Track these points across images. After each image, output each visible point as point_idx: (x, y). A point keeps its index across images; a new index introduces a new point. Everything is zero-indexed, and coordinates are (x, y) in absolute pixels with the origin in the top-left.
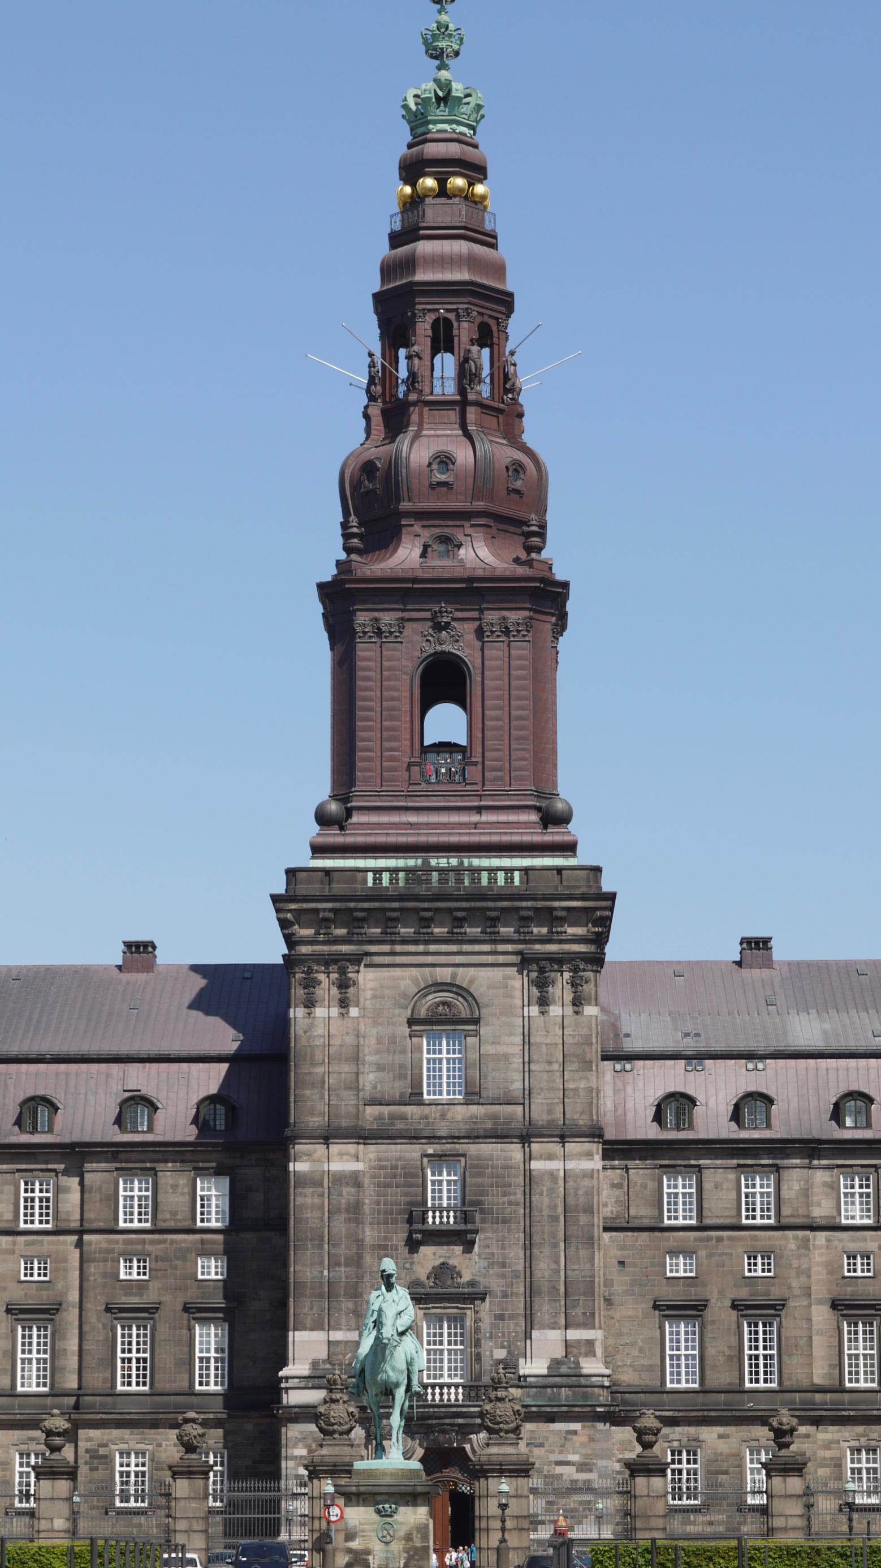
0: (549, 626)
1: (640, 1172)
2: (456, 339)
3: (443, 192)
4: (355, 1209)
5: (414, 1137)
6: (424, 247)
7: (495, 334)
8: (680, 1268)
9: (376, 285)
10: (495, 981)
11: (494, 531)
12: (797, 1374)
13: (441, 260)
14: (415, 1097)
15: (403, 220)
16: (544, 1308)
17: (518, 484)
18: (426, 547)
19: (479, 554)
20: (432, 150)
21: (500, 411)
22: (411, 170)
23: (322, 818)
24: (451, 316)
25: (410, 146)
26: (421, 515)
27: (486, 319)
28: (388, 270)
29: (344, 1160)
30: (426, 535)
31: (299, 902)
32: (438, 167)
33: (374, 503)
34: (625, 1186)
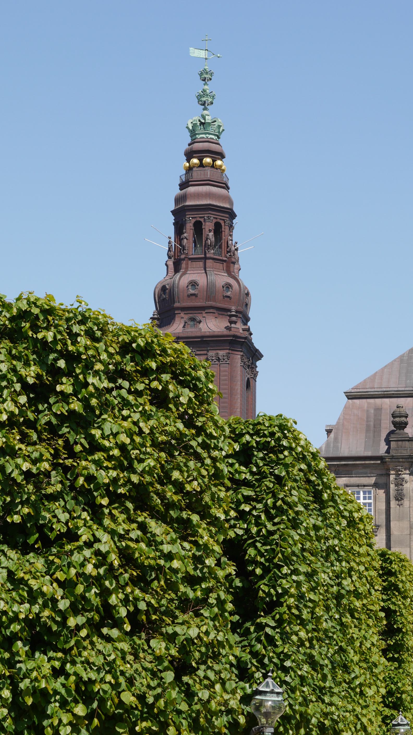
0: (239, 357)
2: (223, 233)
3: (201, 165)
6: (191, 189)
7: (223, 227)
9: (172, 207)
11: (216, 315)
13: (199, 194)
15: (185, 178)
17: (229, 294)
18: (185, 323)
19: (212, 325)
20: (197, 146)
21: (225, 261)
22: (189, 155)
24: (202, 220)
25: (189, 145)
26: (183, 309)
27: (218, 220)
30: (186, 317)
32: (203, 155)
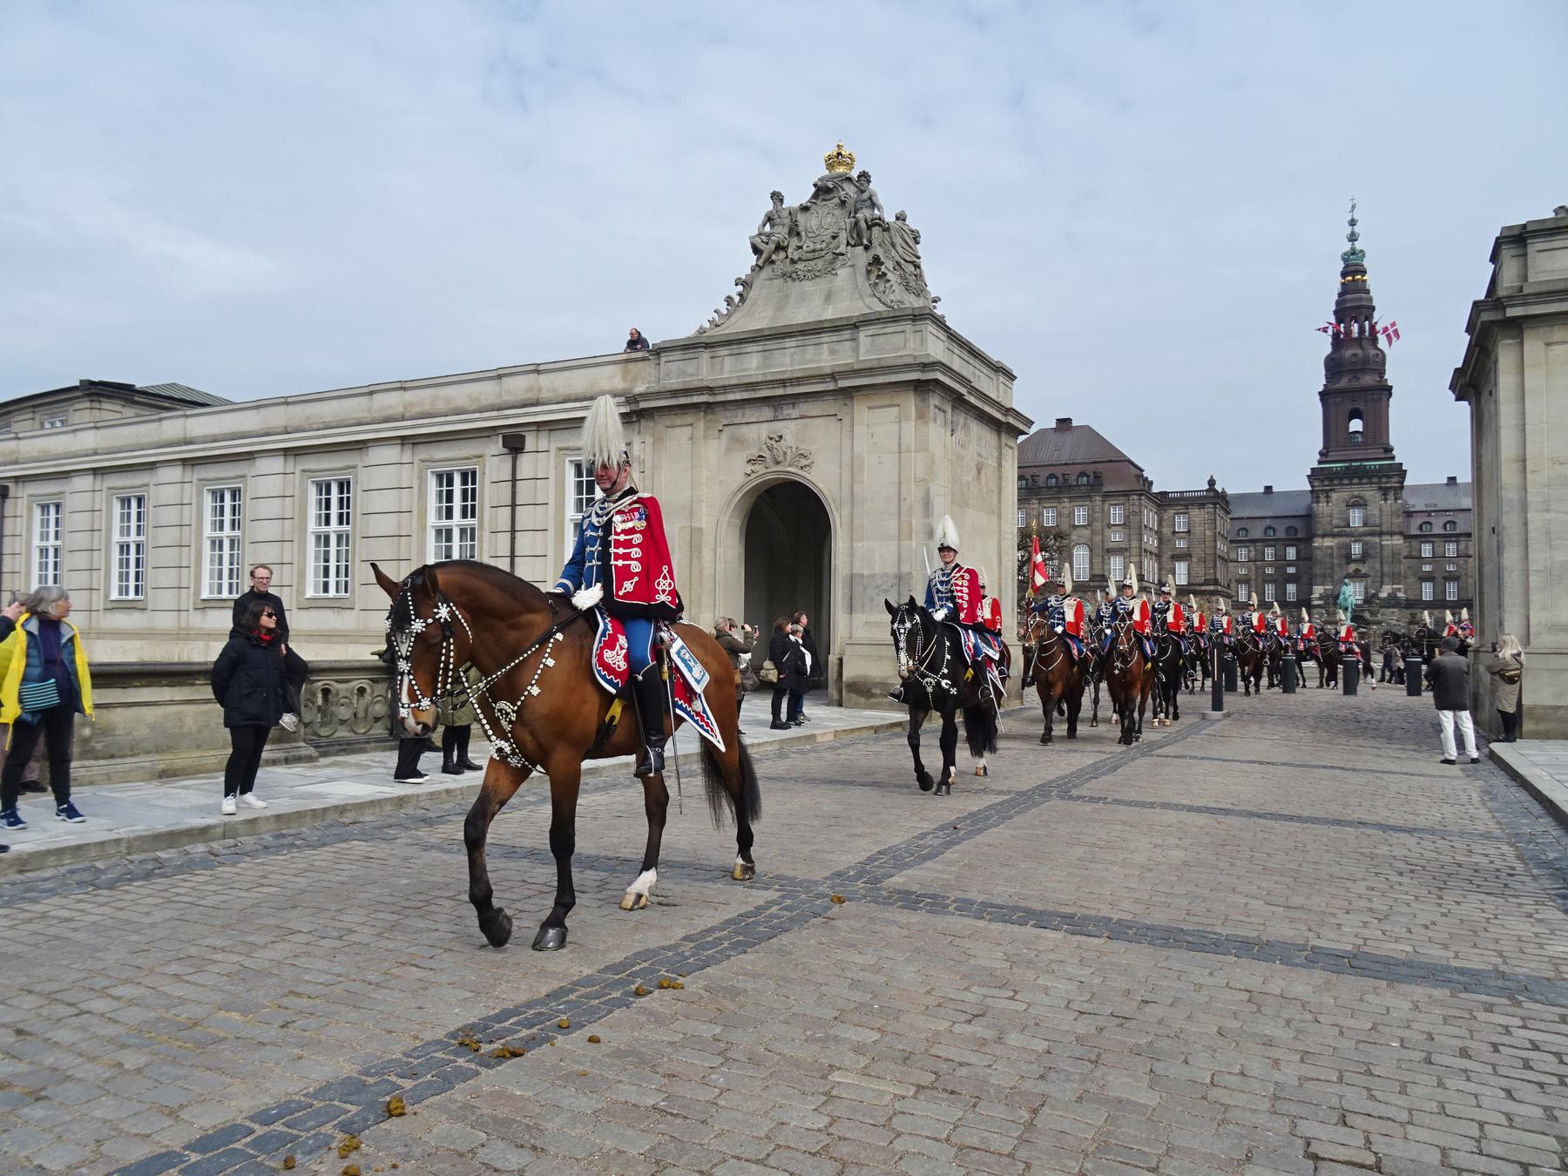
1: (1415, 543)
4: (1331, 555)
5: (1348, 535)
8: (1427, 568)
10: (1370, 493)
12: (1463, 596)
14: (1348, 525)
16: (1386, 579)
23: (1321, 454)
28: (1338, 303)
29: (1328, 542)
31: (1314, 475)
33: (1333, 366)
34: (1410, 547)
